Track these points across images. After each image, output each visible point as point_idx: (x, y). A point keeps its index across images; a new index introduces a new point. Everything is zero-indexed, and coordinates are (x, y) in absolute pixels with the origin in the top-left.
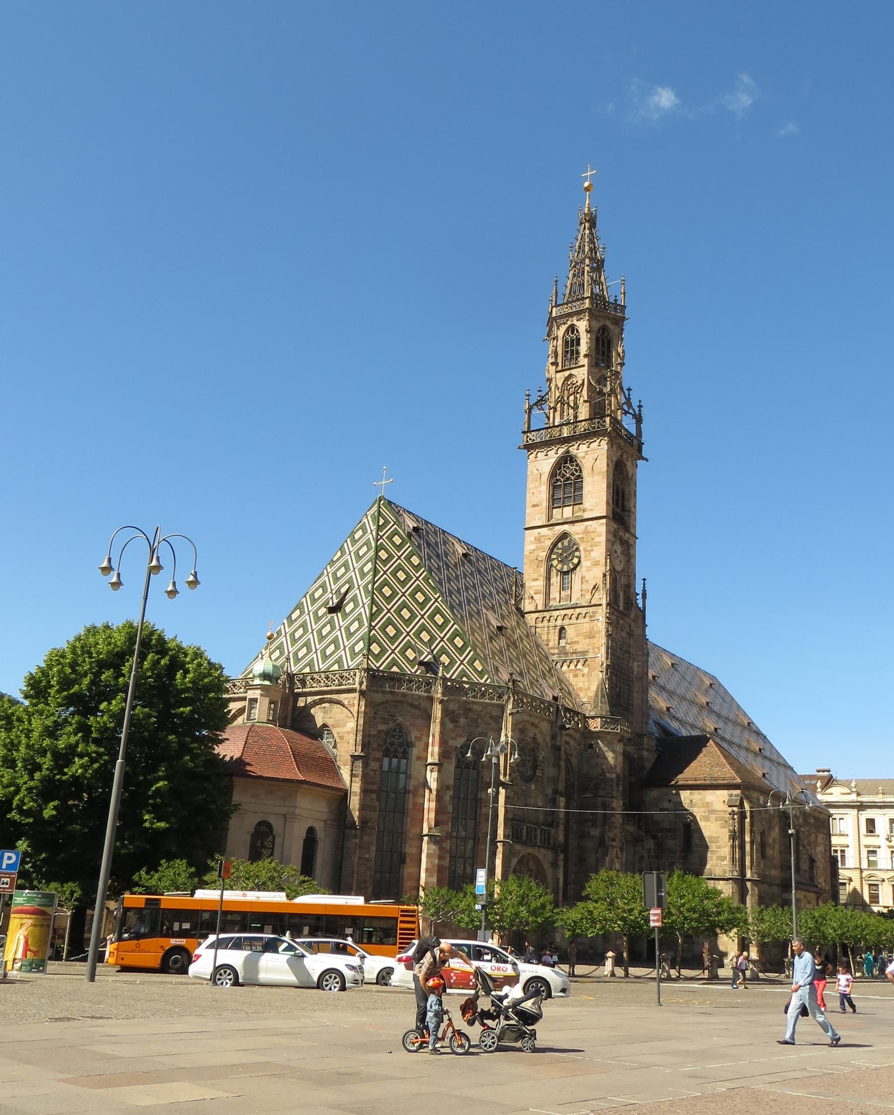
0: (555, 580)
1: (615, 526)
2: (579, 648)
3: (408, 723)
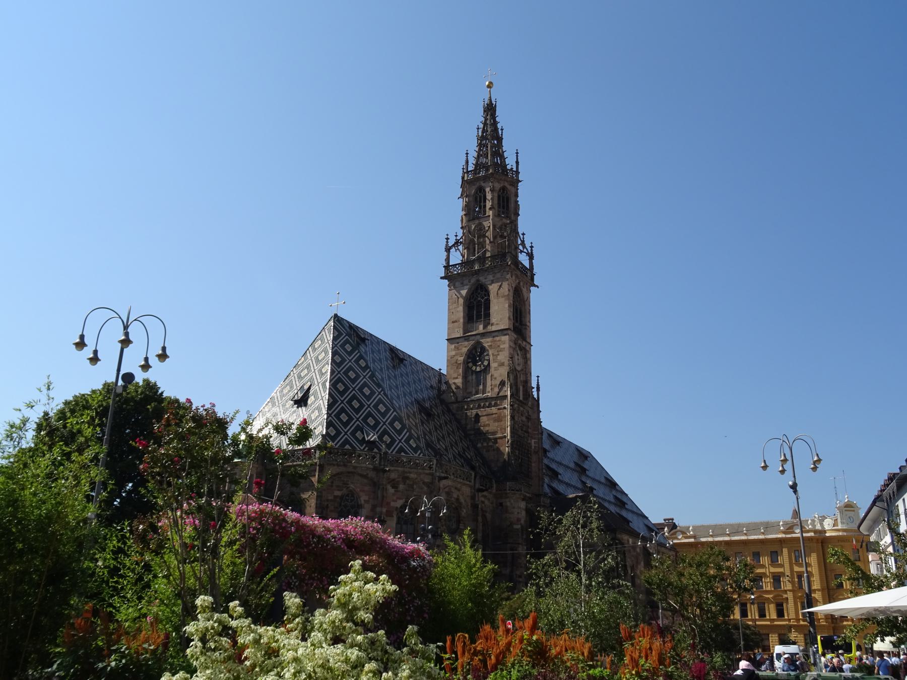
1: (515, 336)
3: (359, 490)
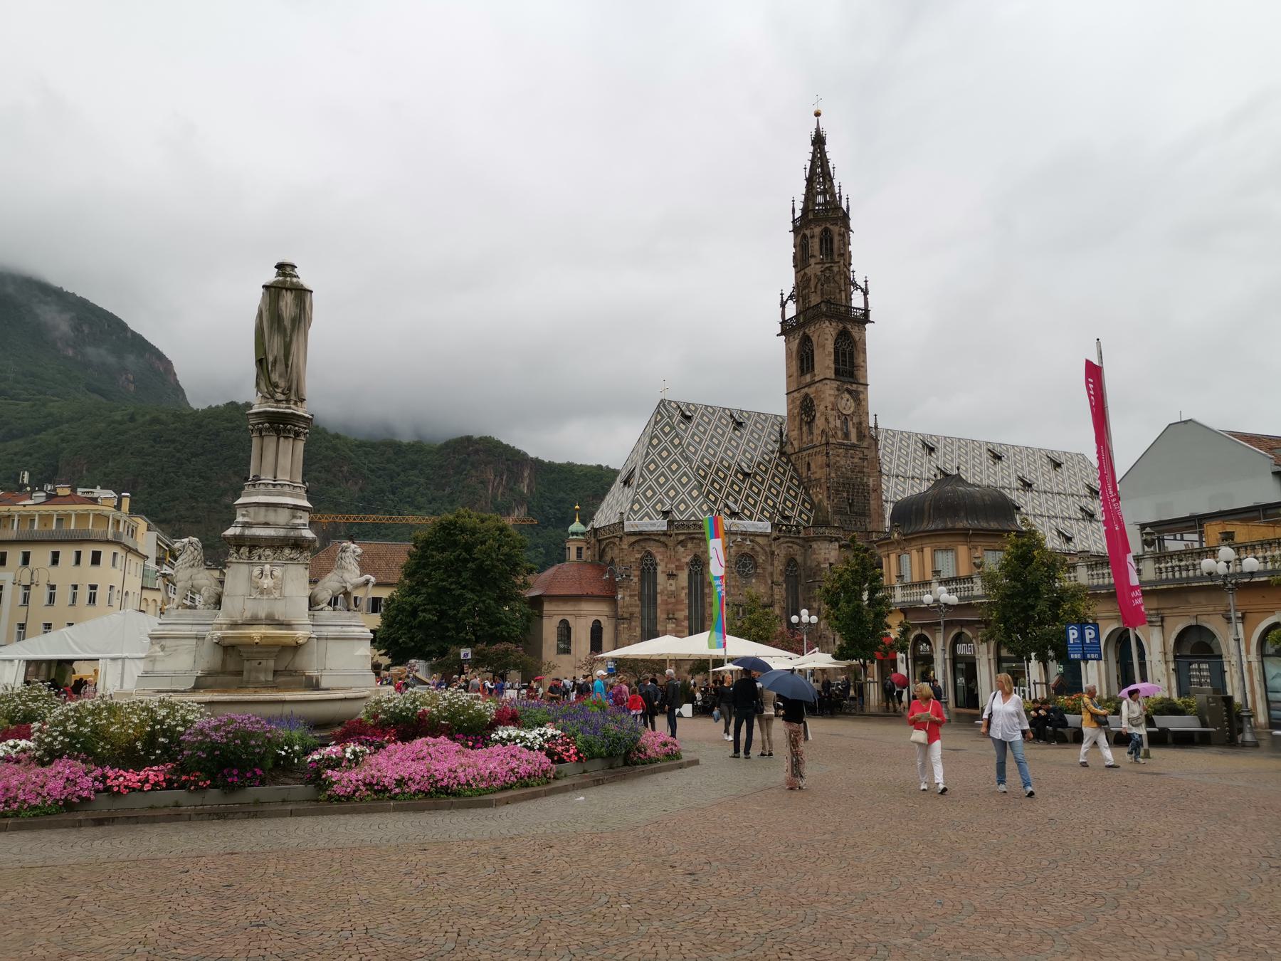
0: (805, 428)
1: (838, 383)
2: (817, 476)
